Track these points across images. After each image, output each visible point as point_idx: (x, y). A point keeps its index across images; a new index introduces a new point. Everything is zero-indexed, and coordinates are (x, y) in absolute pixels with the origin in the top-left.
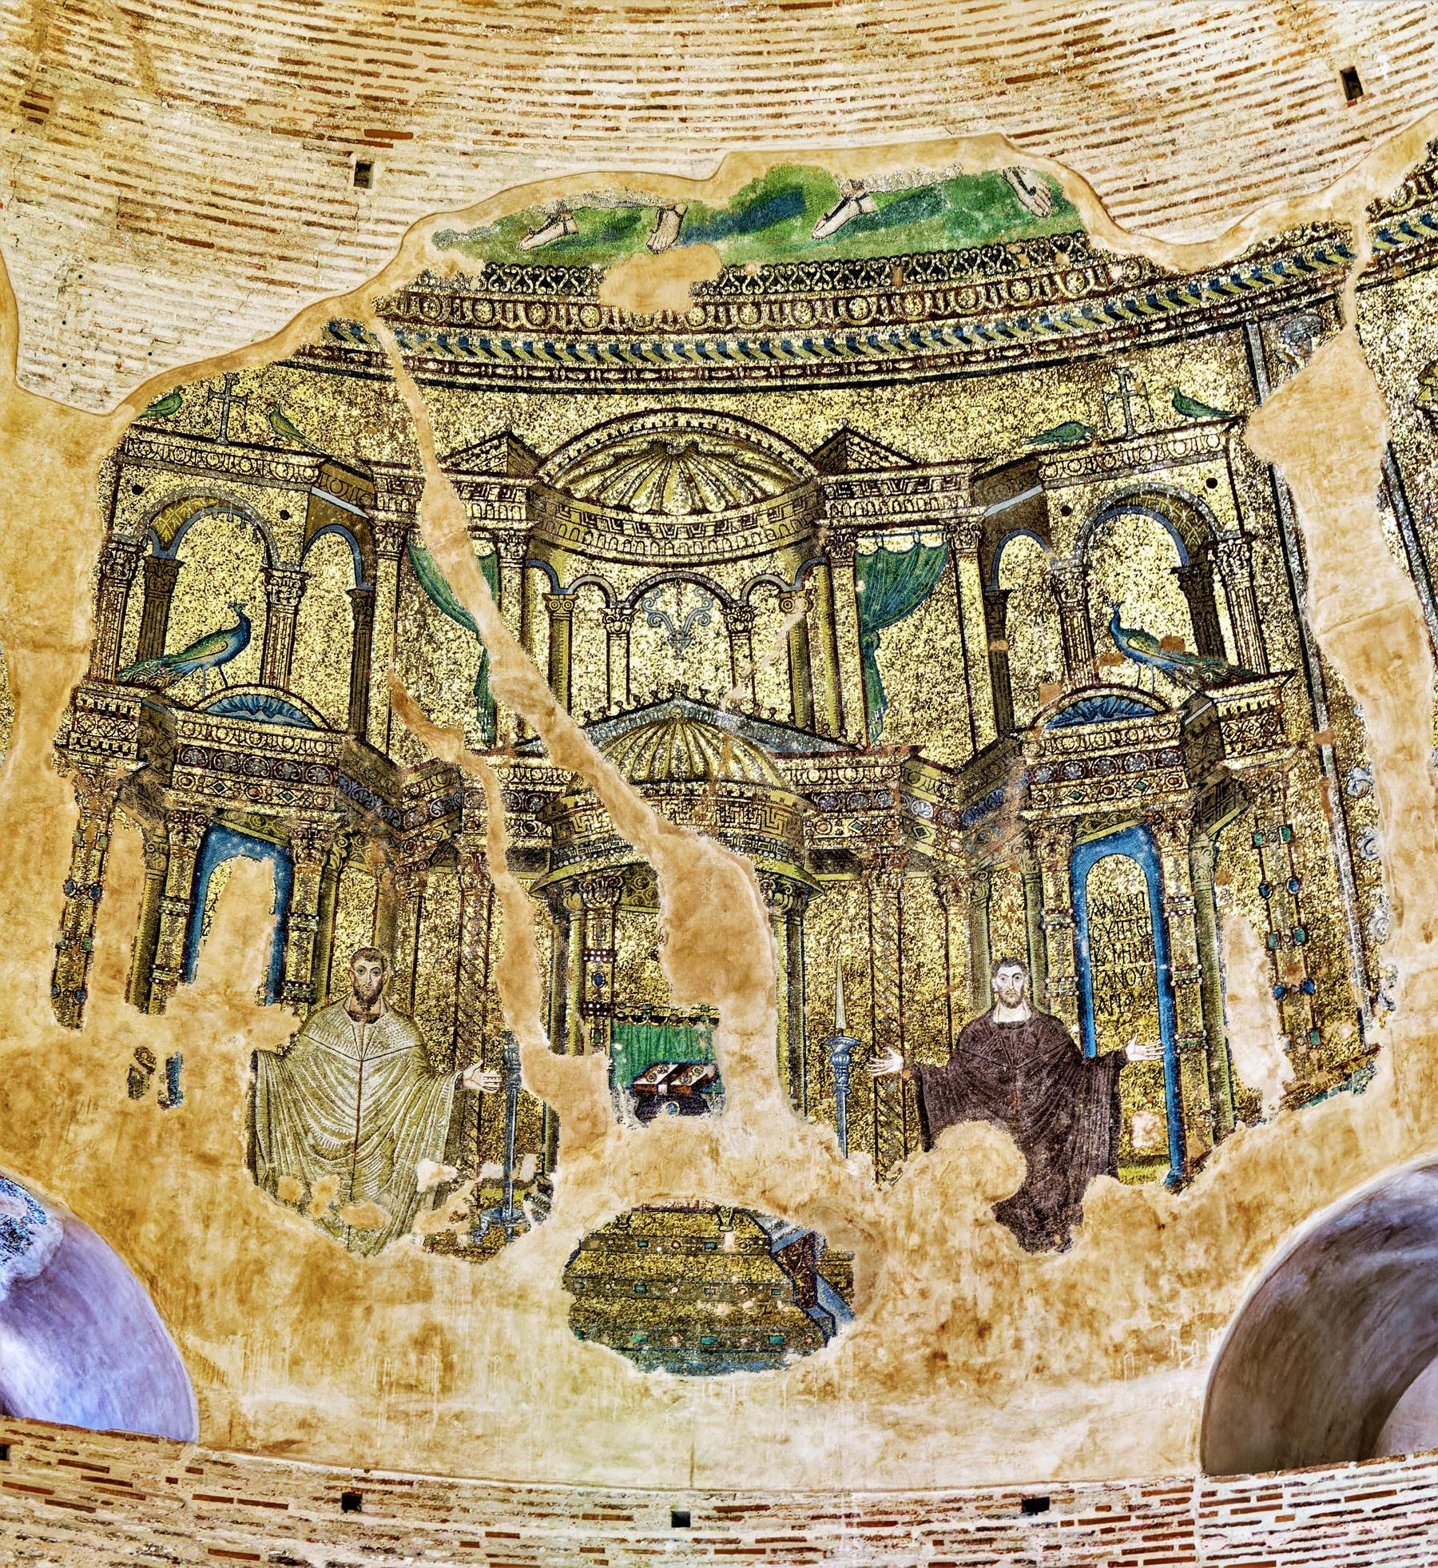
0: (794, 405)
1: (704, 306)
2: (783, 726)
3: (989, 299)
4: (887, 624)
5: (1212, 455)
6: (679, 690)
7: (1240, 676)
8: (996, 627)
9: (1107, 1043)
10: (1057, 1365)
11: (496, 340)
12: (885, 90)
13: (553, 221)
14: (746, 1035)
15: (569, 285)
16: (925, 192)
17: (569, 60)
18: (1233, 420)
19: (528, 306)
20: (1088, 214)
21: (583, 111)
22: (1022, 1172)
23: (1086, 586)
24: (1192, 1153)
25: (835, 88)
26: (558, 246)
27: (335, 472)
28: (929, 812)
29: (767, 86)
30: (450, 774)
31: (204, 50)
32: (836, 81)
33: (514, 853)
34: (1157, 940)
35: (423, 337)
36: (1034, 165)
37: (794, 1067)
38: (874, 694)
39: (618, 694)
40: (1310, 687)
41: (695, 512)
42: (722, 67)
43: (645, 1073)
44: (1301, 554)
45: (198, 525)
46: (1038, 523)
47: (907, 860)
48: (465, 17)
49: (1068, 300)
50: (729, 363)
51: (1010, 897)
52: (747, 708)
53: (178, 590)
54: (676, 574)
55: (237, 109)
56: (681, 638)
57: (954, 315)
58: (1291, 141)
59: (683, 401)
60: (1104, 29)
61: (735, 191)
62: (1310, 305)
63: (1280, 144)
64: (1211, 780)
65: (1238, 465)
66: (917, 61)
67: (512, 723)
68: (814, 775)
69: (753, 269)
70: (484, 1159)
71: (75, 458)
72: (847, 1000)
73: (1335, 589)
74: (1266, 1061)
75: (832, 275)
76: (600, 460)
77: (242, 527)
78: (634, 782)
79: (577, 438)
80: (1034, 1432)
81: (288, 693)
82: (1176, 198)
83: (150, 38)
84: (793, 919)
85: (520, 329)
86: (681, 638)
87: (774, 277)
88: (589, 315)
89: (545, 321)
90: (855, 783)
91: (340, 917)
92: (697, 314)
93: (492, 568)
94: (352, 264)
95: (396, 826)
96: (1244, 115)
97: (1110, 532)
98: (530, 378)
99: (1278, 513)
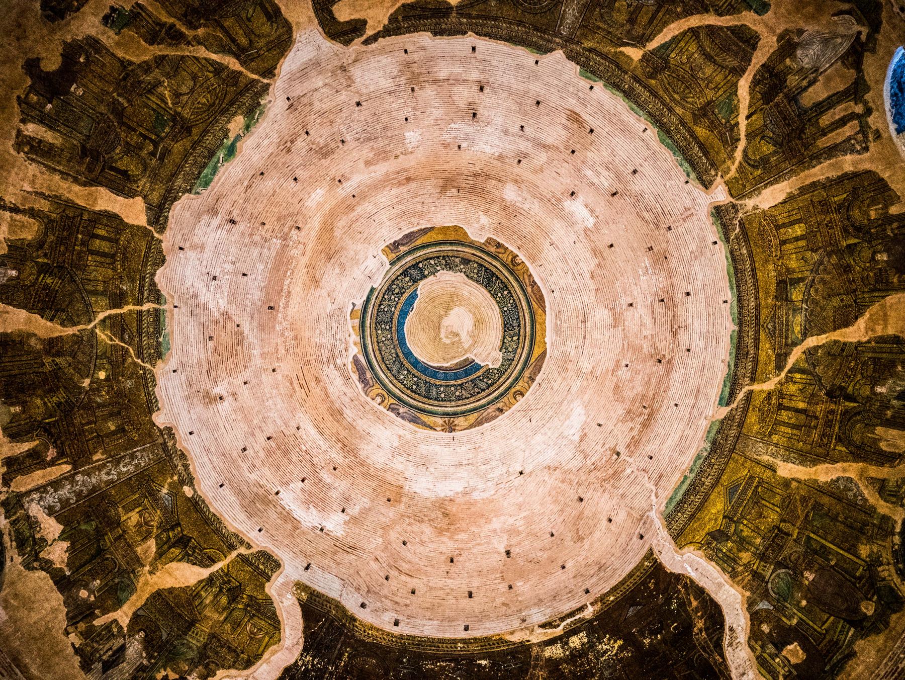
5: (142, 190)
7: (103, 170)
8: (141, 134)
9: (55, 102)
20: (192, 196)
22: (42, 68)
30: (196, 28)
36: (205, 193)
42: (255, 159)
43: (119, 15)
69: (225, 141)
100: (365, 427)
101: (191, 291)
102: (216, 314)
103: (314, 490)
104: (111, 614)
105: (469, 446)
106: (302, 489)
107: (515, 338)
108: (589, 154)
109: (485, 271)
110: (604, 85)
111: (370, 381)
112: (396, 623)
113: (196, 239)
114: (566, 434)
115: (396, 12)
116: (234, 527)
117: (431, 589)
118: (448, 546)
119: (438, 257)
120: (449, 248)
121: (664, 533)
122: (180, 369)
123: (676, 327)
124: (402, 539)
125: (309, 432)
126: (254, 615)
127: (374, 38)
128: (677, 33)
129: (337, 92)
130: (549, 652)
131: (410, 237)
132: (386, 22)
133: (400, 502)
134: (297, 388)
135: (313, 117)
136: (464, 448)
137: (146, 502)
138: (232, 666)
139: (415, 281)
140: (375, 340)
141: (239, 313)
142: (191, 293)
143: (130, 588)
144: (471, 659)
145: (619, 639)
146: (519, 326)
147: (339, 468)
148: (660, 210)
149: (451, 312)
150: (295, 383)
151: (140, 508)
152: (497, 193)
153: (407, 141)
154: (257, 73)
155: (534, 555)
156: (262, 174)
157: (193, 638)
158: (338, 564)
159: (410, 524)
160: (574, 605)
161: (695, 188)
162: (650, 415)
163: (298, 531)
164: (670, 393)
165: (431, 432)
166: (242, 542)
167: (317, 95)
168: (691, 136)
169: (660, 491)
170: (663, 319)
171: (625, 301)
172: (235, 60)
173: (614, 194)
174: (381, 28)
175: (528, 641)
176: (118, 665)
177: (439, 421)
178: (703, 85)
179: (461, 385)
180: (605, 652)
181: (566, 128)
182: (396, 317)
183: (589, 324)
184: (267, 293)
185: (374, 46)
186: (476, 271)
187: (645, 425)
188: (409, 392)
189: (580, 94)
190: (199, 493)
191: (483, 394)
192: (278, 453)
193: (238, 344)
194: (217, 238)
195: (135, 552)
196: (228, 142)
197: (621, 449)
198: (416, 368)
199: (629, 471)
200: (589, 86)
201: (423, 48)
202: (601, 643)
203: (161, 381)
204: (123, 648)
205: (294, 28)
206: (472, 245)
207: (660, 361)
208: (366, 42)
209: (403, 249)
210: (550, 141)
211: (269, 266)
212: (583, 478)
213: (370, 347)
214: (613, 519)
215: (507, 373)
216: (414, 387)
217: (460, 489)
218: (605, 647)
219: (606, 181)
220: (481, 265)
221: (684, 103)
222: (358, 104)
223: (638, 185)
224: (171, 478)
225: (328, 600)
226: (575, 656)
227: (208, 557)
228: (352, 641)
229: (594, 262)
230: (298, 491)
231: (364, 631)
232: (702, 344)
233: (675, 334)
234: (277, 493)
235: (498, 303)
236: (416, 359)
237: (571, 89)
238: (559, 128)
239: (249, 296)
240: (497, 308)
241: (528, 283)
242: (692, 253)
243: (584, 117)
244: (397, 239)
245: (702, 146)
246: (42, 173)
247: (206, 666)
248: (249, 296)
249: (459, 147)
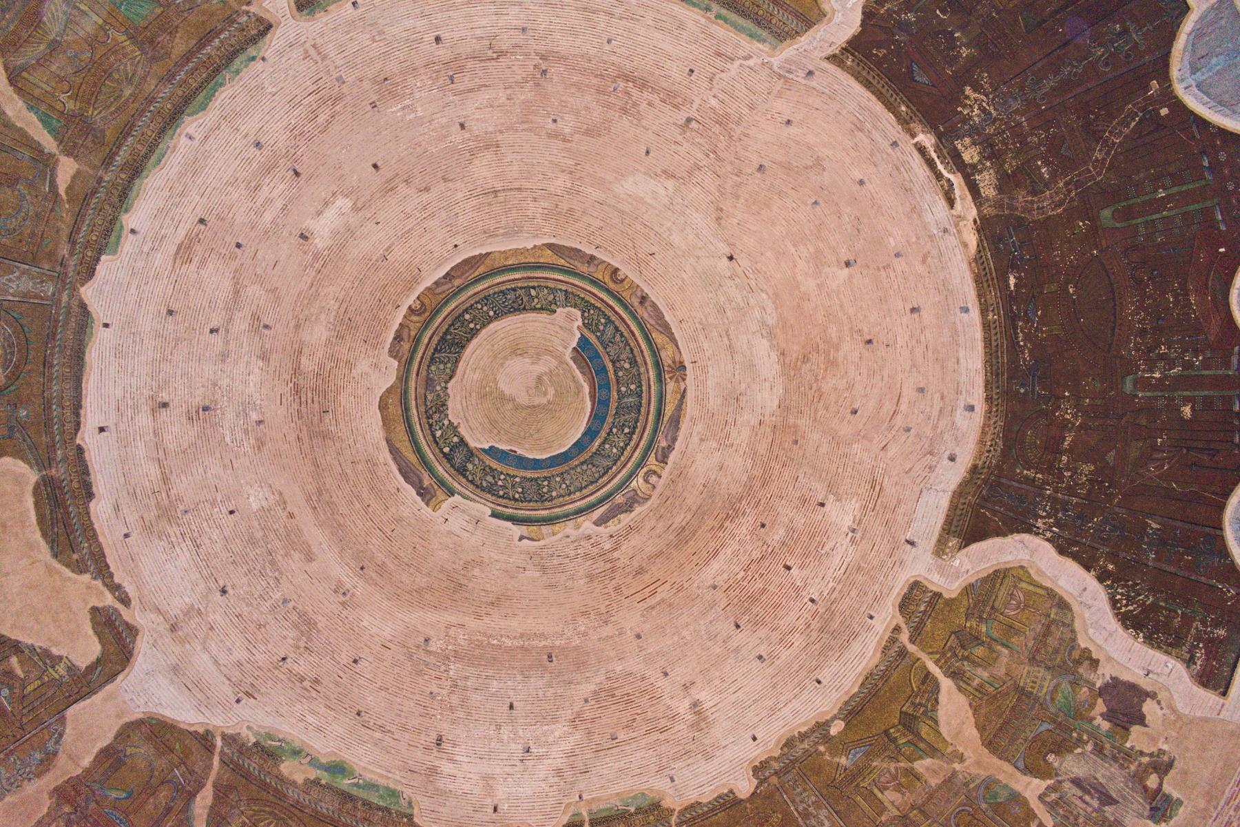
11: (247, 761)
13: (279, 741)
16: (377, 786)
20: (416, 811)
21: (302, 719)
31: (221, 646)
36: (407, 792)
42: (341, 730)
60: (439, 769)
69: (323, 782)
71: (118, 716)
83: (211, 633)
87: (328, 787)
100: (696, 493)
101: (552, 780)
102: (578, 736)
103: (799, 550)
104: (1032, 806)
105: (702, 338)
106: (802, 567)
107: (533, 292)
108: (239, 219)
109: (440, 351)
110: (127, 211)
111: (629, 495)
112: (971, 408)
113: (478, 790)
114: (665, 200)
115: (67, 566)
116: (874, 654)
117: (914, 365)
118: (850, 350)
119: (431, 426)
120: (415, 411)
121: (804, 41)
122: (667, 772)
123: (490, 53)
124: (849, 416)
125: (716, 570)
126: (993, 608)
127: (115, 588)
128: (21, 103)
129: (212, 628)
130: (988, 191)
131: (407, 474)
132: (86, 577)
133: (796, 426)
134: (658, 598)
135: (258, 656)
136: (706, 345)
137: (865, 785)
138: (1070, 626)
139: (471, 454)
140: (567, 498)
141: (567, 704)
142: (556, 779)
143: (989, 784)
144: (1010, 299)
145: (963, 92)
146: (514, 290)
147: (762, 519)
148: (311, 98)
149: (507, 392)
150: (651, 602)
151: (876, 791)
152: (320, 354)
153: (264, 503)
154: (211, 759)
155: (849, 227)
157: (1042, 687)
158: (899, 502)
159: (827, 408)
160: (917, 161)
161: (273, 43)
162: (627, 78)
163: (862, 565)
164: (592, 52)
165: (690, 395)
166: (893, 640)
168: (188, 60)
169: (741, 53)
170: (480, 74)
171: (457, 136)
172: (198, 798)
173: (297, 174)
174: (99, 583)
175: (975, 221)
176: (1101, 784)
177: (671, 386)
178: (102, 50)
179: (613, 362)
180: (983, 110)
181: (203, 263)
182: (529, 474)
183: (499, 186)
184: (531, 667)
185: (130, 589)
186: (442, 366)
187: (643, 85)
188: (635, 437)
189: (146, 249)
190: (835, 712)
191: (622, 328)
192: (755, 610)
193: (613, 696)
194: (467, 760)
195: (939, 787)
196: (325, 778)
197: (681, 117)
198: (598, 432)
199: (714, 102)
200: (131, 236)
201: (117, 508)
202: (971, 118)
203: (692, 796)
204: (1077, 782)
205: (127, 720)
206: (403, 378)
207: (544, 72)
208: (125, 601)
209: (427, 481)
210: (227, 284)
211: (491, 673)
212: (729, 168)
213: (578, 504)
214: (786, 118)
215: (587, 298)
216: (627, 430)
217: (765, 343)
218: (976, 111)
219: (276, 188)
220: (432, 360)
221: (137, 79)
222: (224, 592)
223: (277, 136)
224: (822, 754)
225: (953, 507)
226: (992, 153)
227: (923, 683)
228: (1004, 467)
229: (402, 189)
230: (805, 573)
231: (989, 451)
232: (513, 11)
233: (501, 54)
234: (812, 601)
235: (484, 326)
236: (584, 434)
237: (140, 264)
238: (204, 273)
239: (540, 695)
240: (492, 326)
241: (450, 285)
242: (374, 41)
243: (184, 233)
244: (413, 492)
245: (203, 41)
247: (1078, 663)
248: (541, 693)
249: (260, 422)
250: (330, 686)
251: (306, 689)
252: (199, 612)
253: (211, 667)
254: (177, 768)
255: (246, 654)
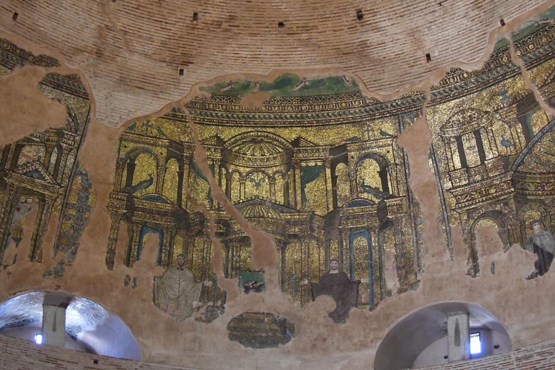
0: (287, 131)
1: (265, 107)
2: (281, 205)
3: (336, 107)
4: (308, 183)
5: (389, 145)
6: (257, 197)
7: (392, 197)
9: (357, 278)
10: (342, 348)
12: (313, 55)
13: (229, 85)
14: (271, 275)
15: (232, 100)
16: (321, 80)
17: (233, 45)
18: (392, 136)
19: (222, 105)
20: (361, 87)
23: (356, 175)
24: (375, 302)
25: (300, 54)
26: (230, 91)
27: (173, 143)
28: (316, 226)
29: (283, 53)
30: (201, 215)
32: (300, 53)
33: (216, 233)
34: (369, 256)
35: (196, 112)
36: (348, 75)
37: (282, 283)
38: (304, 199)
39: (242, 197)
40: (409, 200)
41: (262, 155)
42: (272, 48)
44: (409, 169)
45: (140, 156)
46: (345, 160)
47: (311, 237)
48: (208, 34)
49: (356, 108)
50: (271, 120)
51: (334, 245)
52: (273, 201)
53: (136, 170)
54: (257, 170)
55: (150, 55)
56: (258, 185)
57: (327, 110)
58: (413, 71)
59: (260, 129)
61: (275, 78)
62: (415, 110)
63: (409, 72)
64: (384, 220)
65: (395, 148)
66: (321, 48)
67: (216, 203)
68: (289, 217)
70: (209, 301)
72: (295, 268)
73: (416, 177)
74: (393, 283)
75: (297, 100)
76: (239, 143)
77: (151, 156)
78: (246, 218)
79: (233, 137)
80: (336, 362)
81: (162, 195)
82: (384, 84)
84: (283, 249)
85: (220, 111)
86: (258, 185)
88: (237, 108)
89: (226, 109)
90: (299, 219)
91: (175, 247)
92: (264, 108)
93: (212, 167)
94: (179, 94)
95: (188, 227)
96: (402, 64)
97: (363, 163)
98: (222, 123)
99: (404, 160)
113: (408, 48)
129: (125, 33)
156: (281, 24)
167: (150, 49)
246: (427, 250)
250: (245, 15)
251: (226, 30)
252: (108, 28)
253: (146, 62)
254: (170, 147)
255: (164, 34)
